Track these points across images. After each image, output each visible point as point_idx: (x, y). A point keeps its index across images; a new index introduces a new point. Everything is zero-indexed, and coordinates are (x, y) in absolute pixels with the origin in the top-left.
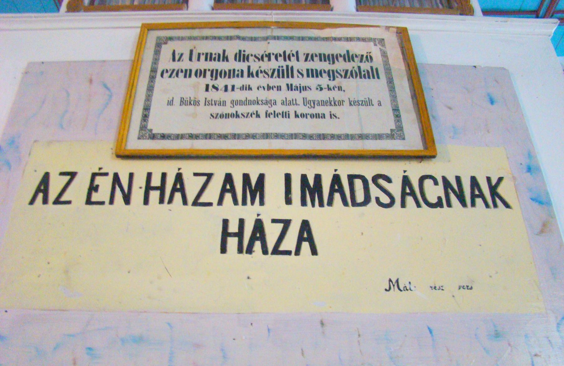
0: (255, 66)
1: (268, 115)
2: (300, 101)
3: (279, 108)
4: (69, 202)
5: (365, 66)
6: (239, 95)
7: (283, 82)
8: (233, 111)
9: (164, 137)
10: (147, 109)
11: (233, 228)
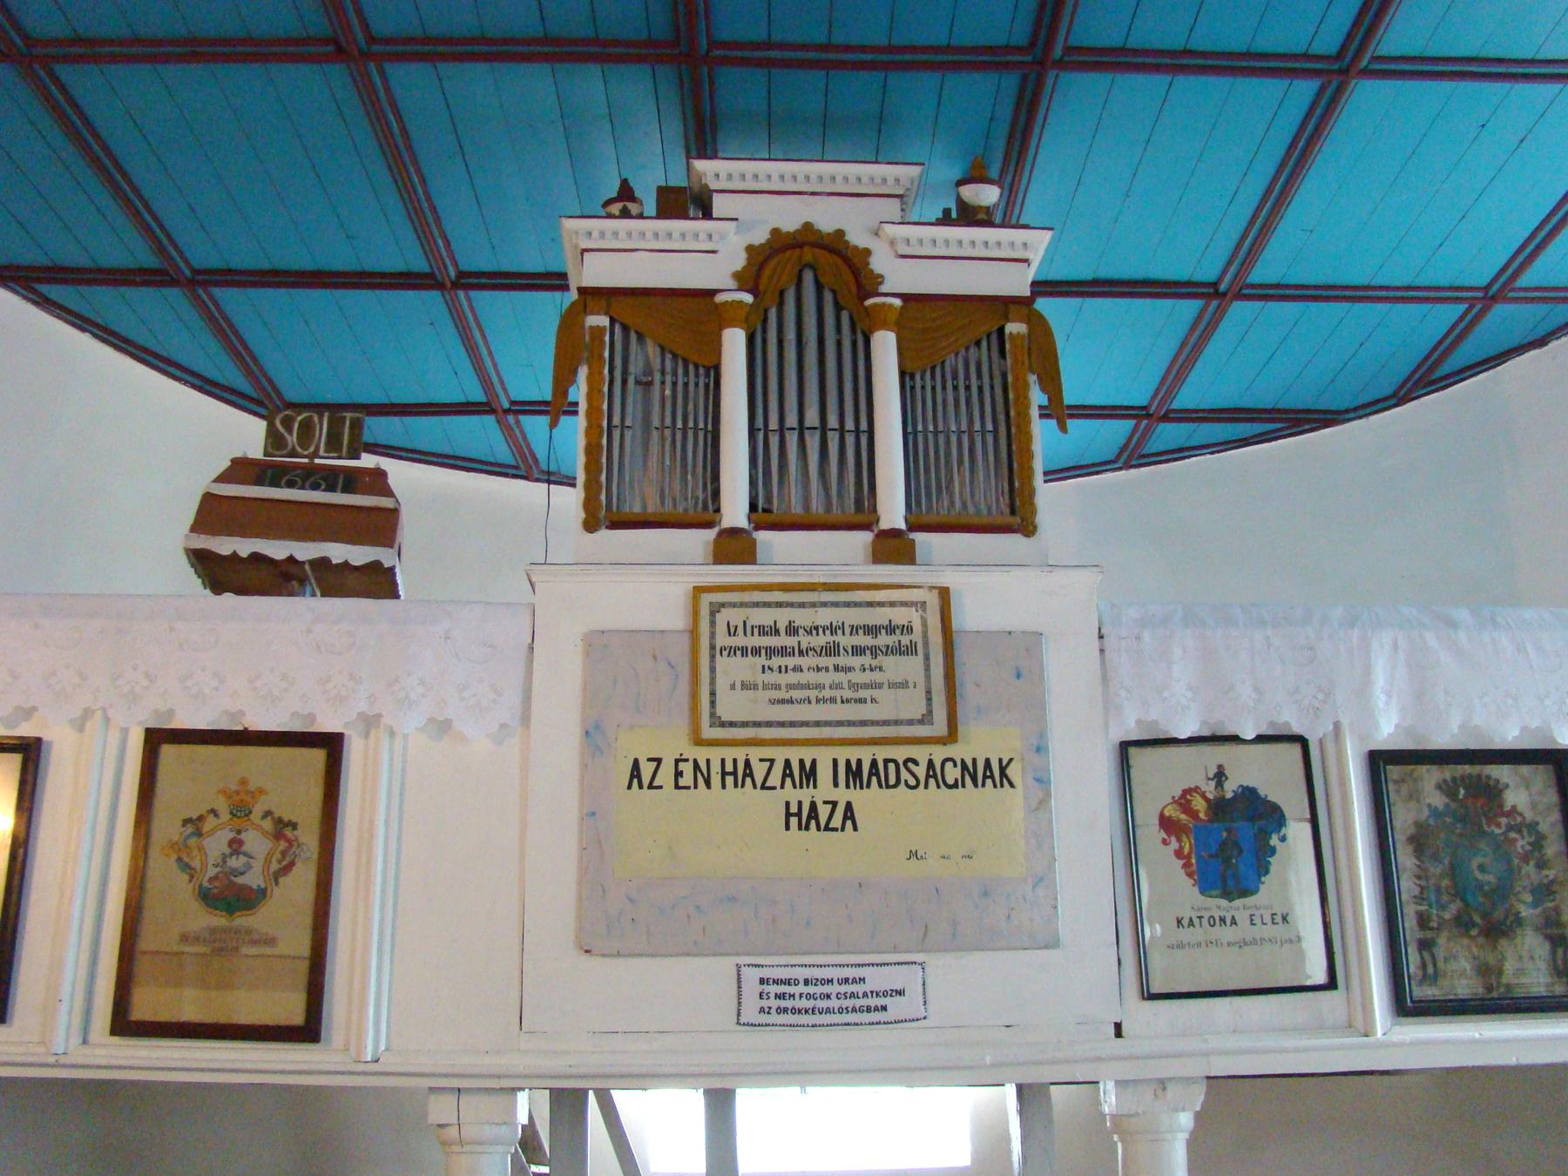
0: (806, 641)
1: (818, 701)
2: (845, 685)
3: (827, 693)
4: (661, 787)
5: (905, 640)
6: (793, 678)
8: (787, 696)
9: (732, 724)
10: (713, 694)
11: (794, 809)
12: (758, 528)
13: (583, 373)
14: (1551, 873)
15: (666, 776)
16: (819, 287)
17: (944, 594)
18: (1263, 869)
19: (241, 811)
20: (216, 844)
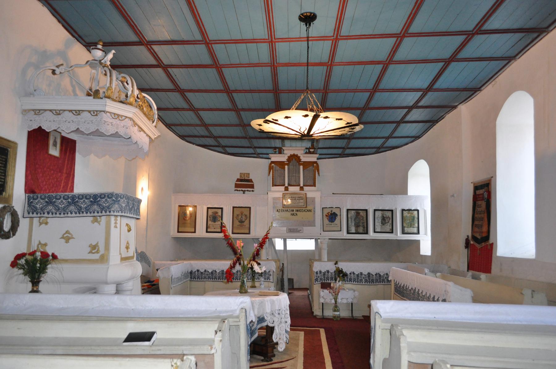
7: (295, 200)
12: (289, 186)
13: (272, 170)
14: (364, 221)
15: (280, 211)
16: (295, 160)
17: (306, 194)
18: (335, 220)
19: (242, 214)
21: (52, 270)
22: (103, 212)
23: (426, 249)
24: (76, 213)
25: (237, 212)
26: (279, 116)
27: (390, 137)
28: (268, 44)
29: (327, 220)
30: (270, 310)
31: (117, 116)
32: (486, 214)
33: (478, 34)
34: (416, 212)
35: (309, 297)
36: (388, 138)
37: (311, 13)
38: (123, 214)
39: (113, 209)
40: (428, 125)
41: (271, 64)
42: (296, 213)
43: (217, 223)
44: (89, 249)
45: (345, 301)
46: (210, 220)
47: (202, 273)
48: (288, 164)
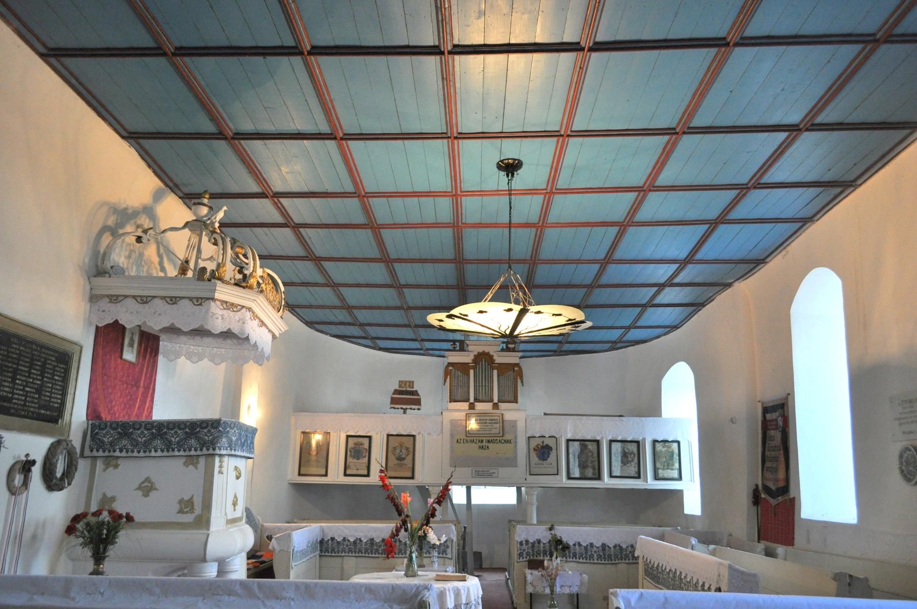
12: (475, 402)
13: (449, 377)
15: (462, 441)
17: (502, 414)
18: (549, 457)
20: (398, 451)
21: (125, 538)
22: (204, 449)
23: (693, 505)
24: (162, 451)
25: (394, 442)
26: (469, 309)
27: (633, 326)
28: (451, 198)
29: (535, 456)
30: (453, 605)
31: (229, 306)
32: (782, 452)
33: (755, 188)
34: (675, 445)
35: (507, 584)
36: (628, 328)
37: (515, 160)
38: (233, 452)
39: (219, 445)
40: (690, 309)
41: (454, 224)
42: (487, 444)
43: (361, 461)
44: (177, 507)
45: (567, 591)
46: (351, 455)
47: (338, 543)
48: (474, 368)
